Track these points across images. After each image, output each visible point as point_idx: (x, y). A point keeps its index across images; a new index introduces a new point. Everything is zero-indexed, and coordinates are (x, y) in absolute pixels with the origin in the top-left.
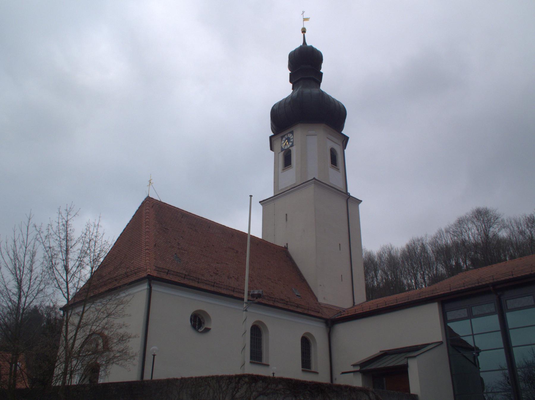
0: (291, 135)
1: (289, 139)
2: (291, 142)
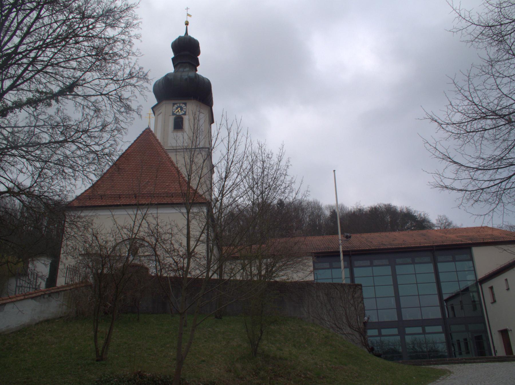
0: (183, 105)
1: (182, 109)
2: (184, 111)
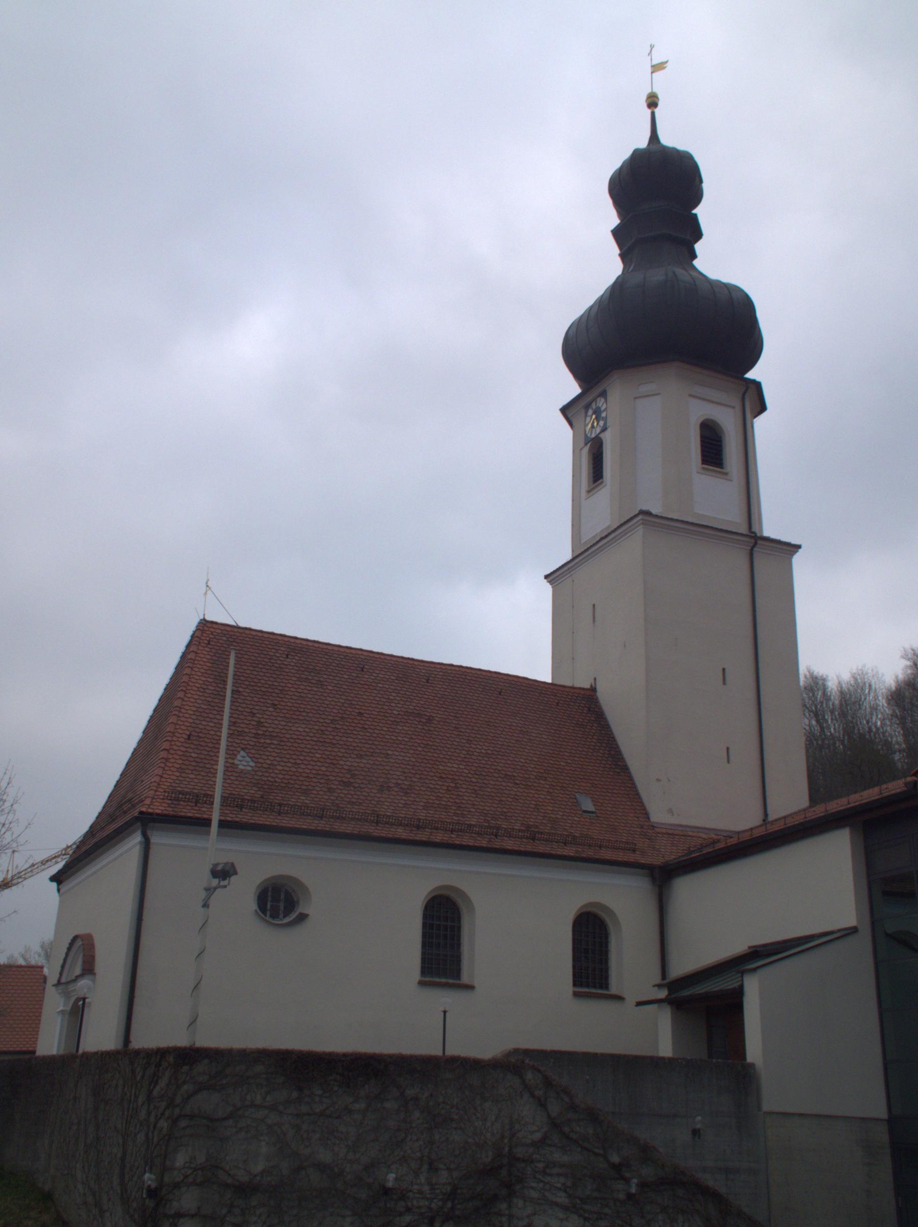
1: (598, 412)
2: (603, 419)
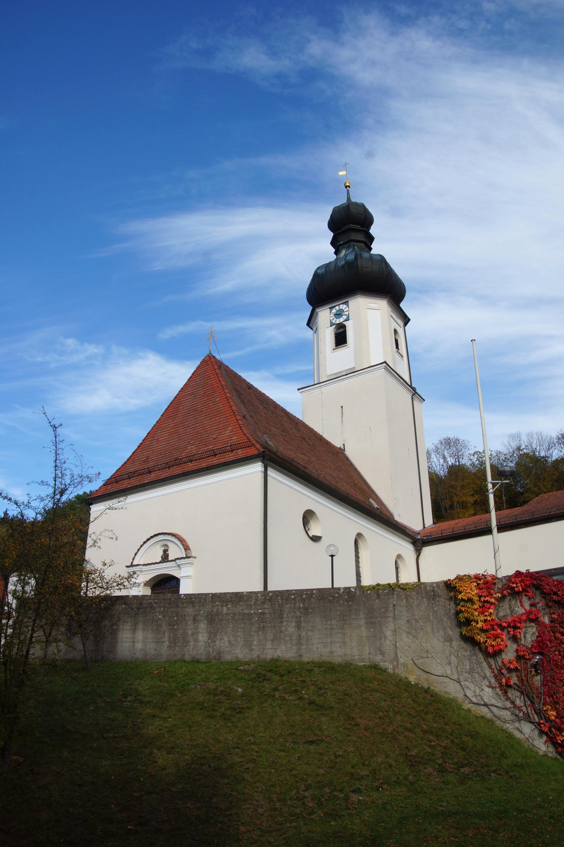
0: (345, 306)
